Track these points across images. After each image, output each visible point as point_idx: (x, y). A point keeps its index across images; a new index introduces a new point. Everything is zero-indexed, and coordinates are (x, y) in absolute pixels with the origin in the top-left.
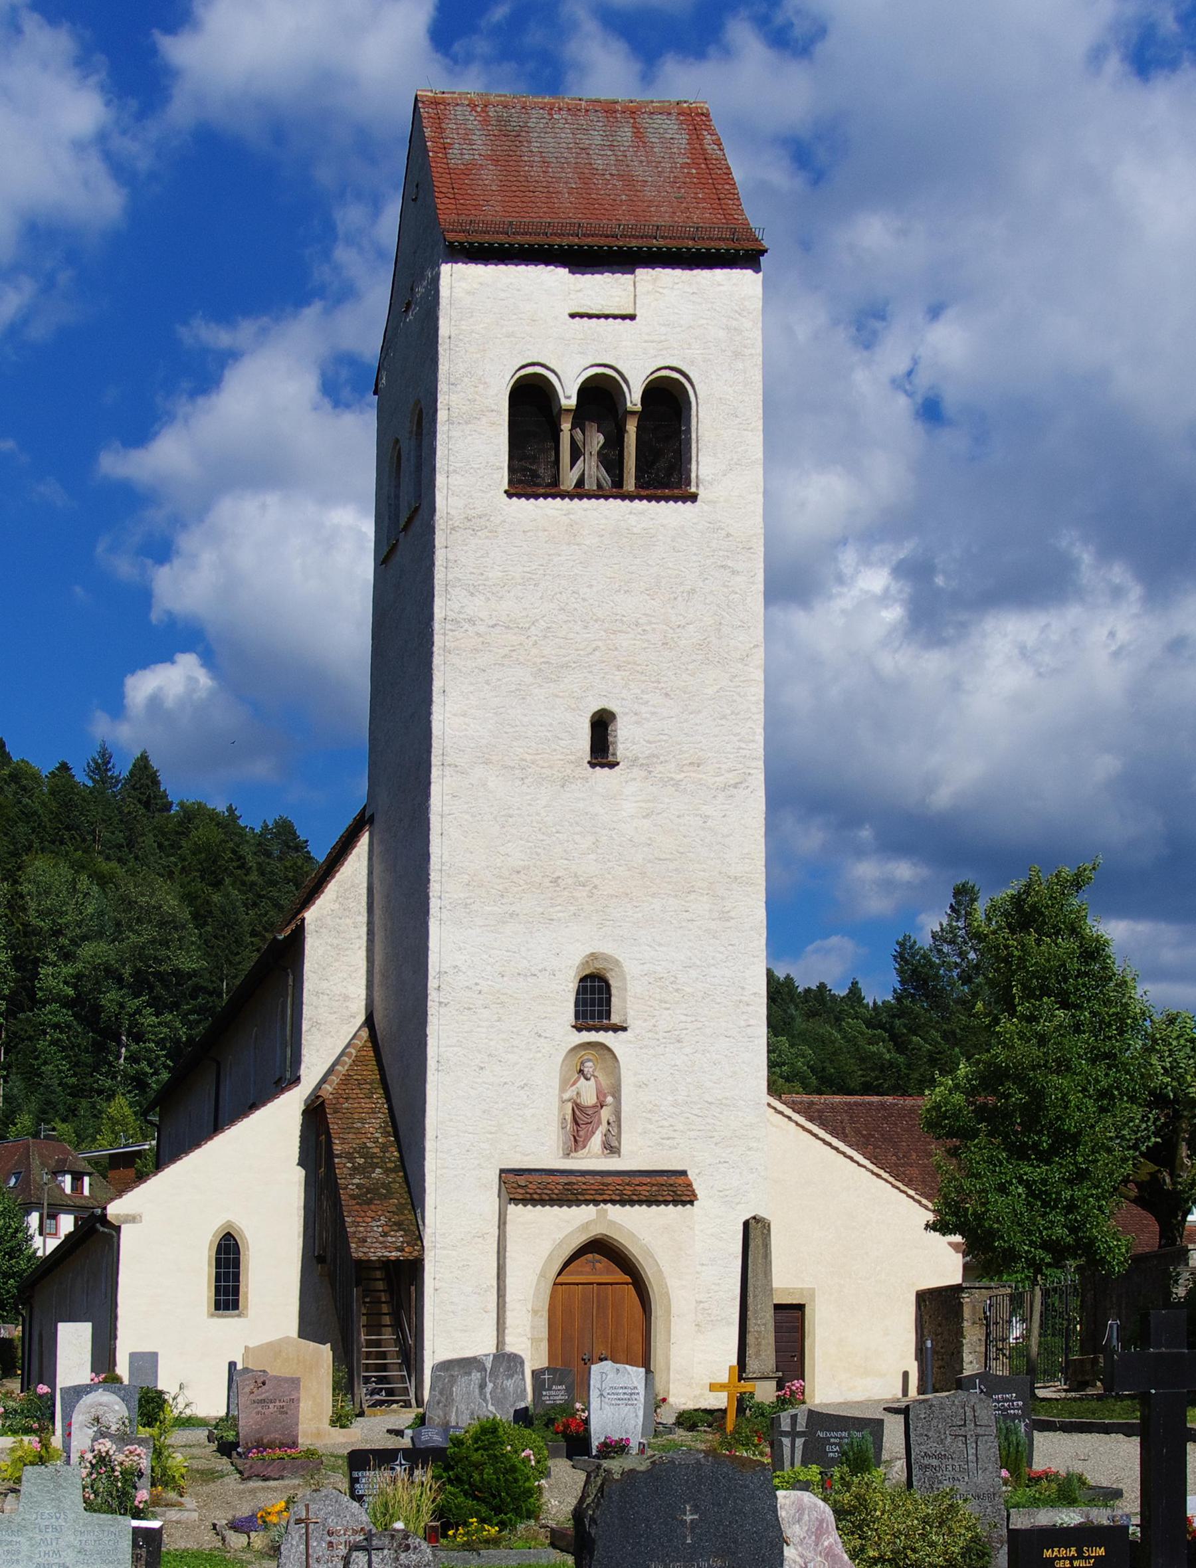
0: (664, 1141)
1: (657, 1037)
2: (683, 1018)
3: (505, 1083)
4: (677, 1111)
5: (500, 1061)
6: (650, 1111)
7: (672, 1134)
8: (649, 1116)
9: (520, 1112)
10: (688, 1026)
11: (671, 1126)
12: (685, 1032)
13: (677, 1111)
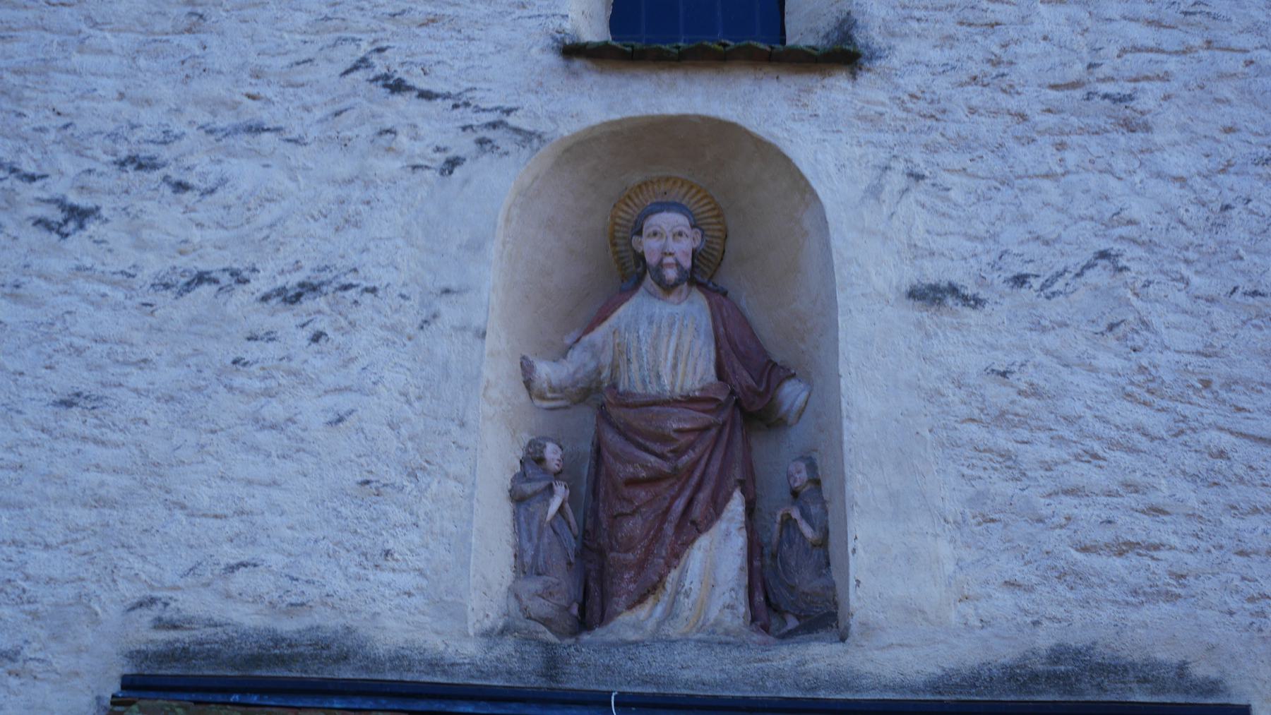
0: (1097, 561)
1: (1012, 103)
2: (1141, 34)
3: (202, 278)
4: (1156, 422)
5: (181, 187)
6: (1001, 418)
7: (1142, 528)
8: (1002, 440)
9: (274, 410)
10: (1172, 64)
11: (1132, 488)
12: (1156, 88)
13: (1156, 422)
